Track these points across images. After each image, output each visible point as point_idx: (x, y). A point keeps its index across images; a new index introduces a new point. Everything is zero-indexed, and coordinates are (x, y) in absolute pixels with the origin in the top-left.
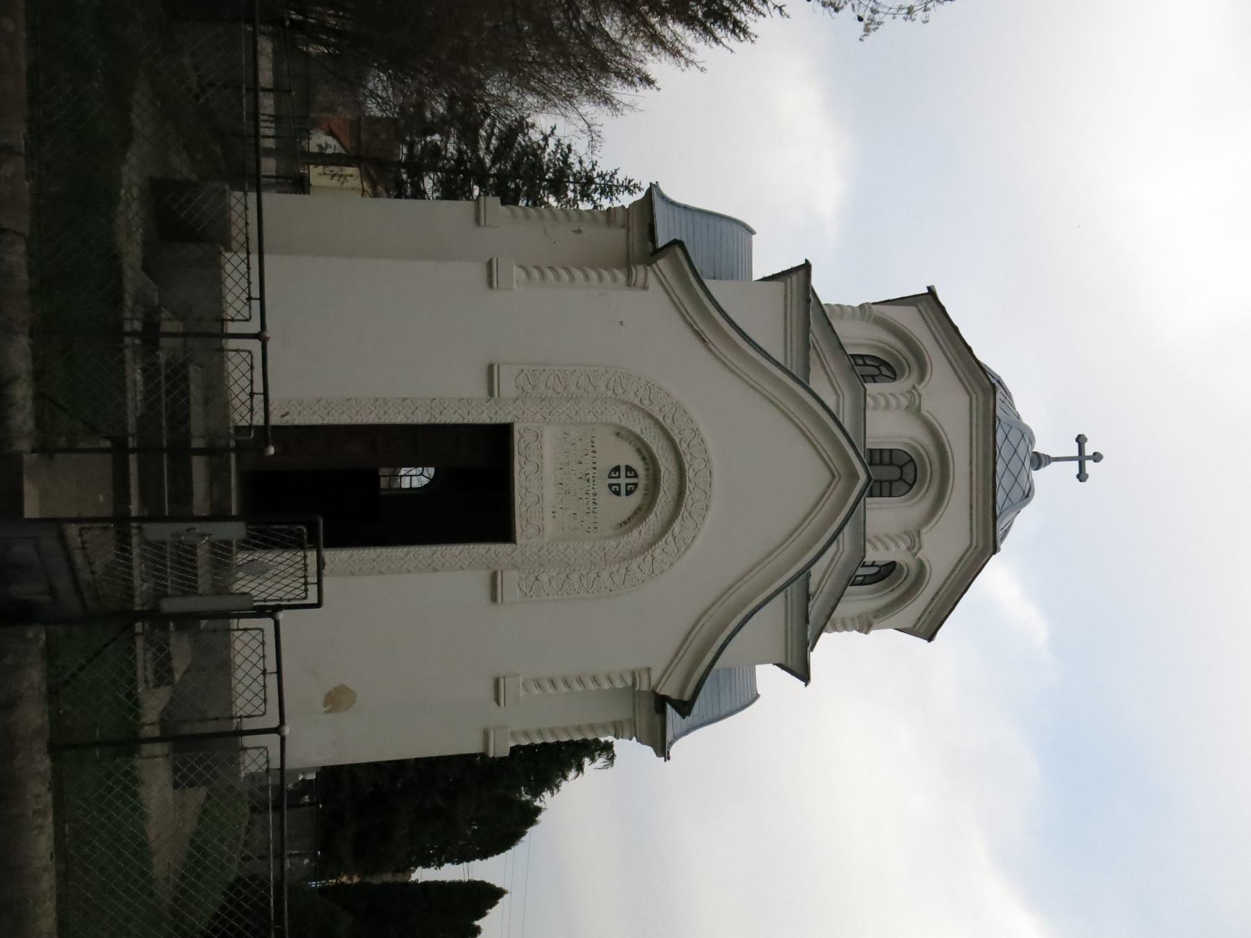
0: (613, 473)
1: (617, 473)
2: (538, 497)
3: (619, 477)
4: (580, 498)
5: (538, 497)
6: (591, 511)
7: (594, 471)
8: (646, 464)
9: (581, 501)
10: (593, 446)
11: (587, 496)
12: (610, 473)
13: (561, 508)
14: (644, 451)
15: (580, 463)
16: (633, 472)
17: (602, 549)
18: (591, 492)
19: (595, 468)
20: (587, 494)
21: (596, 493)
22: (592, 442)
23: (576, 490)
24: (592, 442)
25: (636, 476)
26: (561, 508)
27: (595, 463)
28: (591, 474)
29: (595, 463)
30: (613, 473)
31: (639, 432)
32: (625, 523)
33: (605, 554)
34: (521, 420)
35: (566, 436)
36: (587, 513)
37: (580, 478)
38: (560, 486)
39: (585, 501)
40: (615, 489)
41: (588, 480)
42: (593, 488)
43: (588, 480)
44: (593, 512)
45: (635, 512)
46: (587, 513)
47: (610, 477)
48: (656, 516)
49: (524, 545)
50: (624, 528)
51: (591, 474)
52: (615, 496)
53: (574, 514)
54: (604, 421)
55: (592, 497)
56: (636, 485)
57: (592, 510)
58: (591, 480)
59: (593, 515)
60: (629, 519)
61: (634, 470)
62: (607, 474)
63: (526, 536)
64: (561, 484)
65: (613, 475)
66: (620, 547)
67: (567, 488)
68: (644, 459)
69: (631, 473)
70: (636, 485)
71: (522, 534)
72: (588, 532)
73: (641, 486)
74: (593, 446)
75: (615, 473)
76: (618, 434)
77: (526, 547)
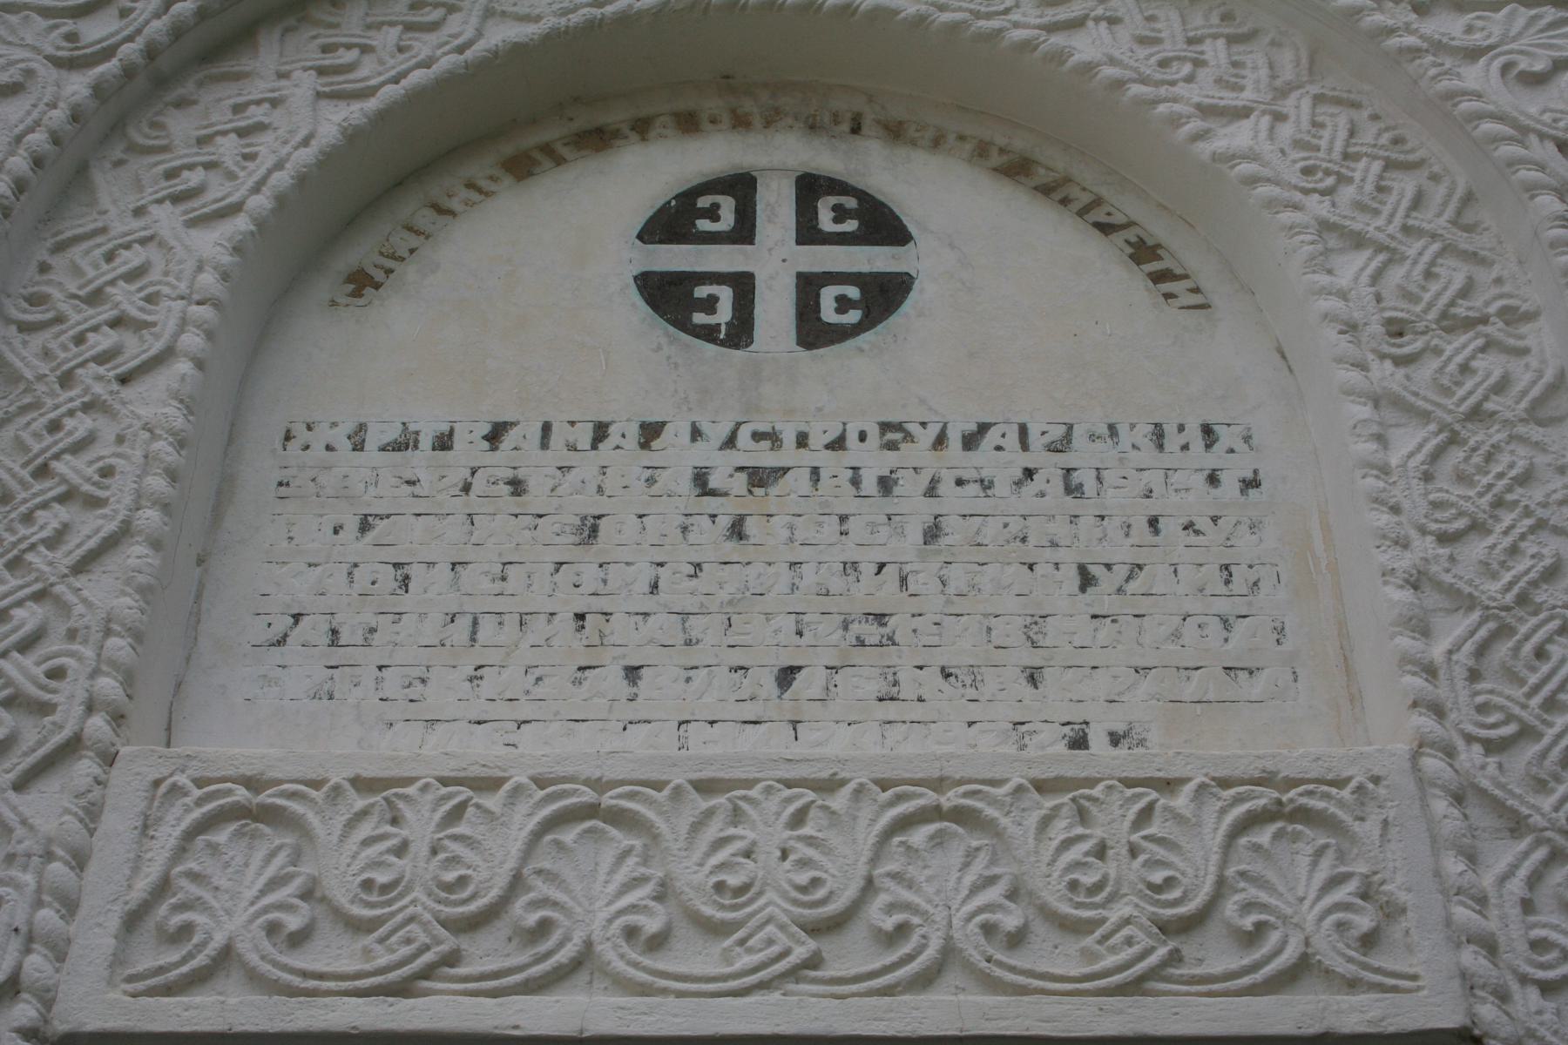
0: (699, 318)
1: (702, 292)
2: (904, 824)
3: (743, 285)
4: (932, 533)
5: (904, 824)
6: (1050, 467)
7: (676, 433)
8: (642, 128)
9: (955, 532)
10: (444, 443)
11: (910, 486)
12: (708, 334)
13: (1033, 678)
14: (531, 140)
15: (590, 530)
16: (704, 202)
17: (1412, 345)
18: (875, 462)
19: (650, 432)
20: (886, 485)
21: (885, 427)
22: (404, 444)
23: (850, 567)
24: (404, 444)
25: (742, 186)
26: (1033, 678)
27: (601, 432)
28: (706, 453)
29: (601, 432)
30: (699, 318)
31: (334, 121)
32: (1143, 252)
33: (1451, 323)
34: (37, 965)
35: (313, 629)
36: (1074, 490)
37: (737, 530)
38: (808, 684)
39: (952, 500)
40: (843, 304)
41: (759, 478)
42: (838, 444)
43: (759, 478)
44: (1059, 446)
45: (1046, 190)
46: (1074, 490)
47: (741, 332)
48: (1077, 24)
49: (1471, 958)
50: (1183, 250)
51: (706, 453)
52: (907, 306)
53: (1086, 580)
54: (205, 312)
55: (919, 452)
56: (810, 188)
57: (1037, 457)
58: (765, 458)
59: (1083, 455)
60: (1105, 228)
61: (687, 198)
62: (711, 349)
63: (1369, 941)
64: (787, 675)
65: (724, 313)
66: (1369, 226)
67: (826, 631)
68: (598, 139)
69: (713, 213)
70: (810, 188)
71: (1353, 985)
72: (1251, 483)
73: (826, 160)
74: (444, 443)
75: (710, 305)
76: (361, 283)
77: (1490, 947)
